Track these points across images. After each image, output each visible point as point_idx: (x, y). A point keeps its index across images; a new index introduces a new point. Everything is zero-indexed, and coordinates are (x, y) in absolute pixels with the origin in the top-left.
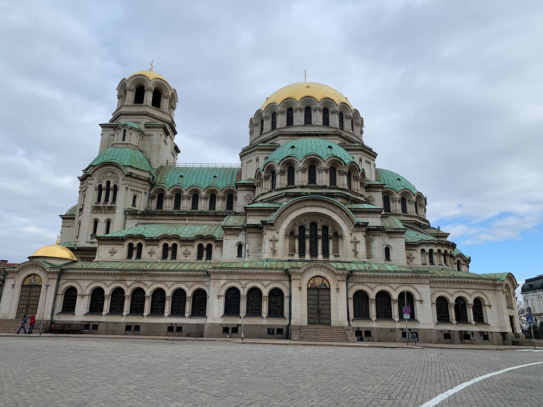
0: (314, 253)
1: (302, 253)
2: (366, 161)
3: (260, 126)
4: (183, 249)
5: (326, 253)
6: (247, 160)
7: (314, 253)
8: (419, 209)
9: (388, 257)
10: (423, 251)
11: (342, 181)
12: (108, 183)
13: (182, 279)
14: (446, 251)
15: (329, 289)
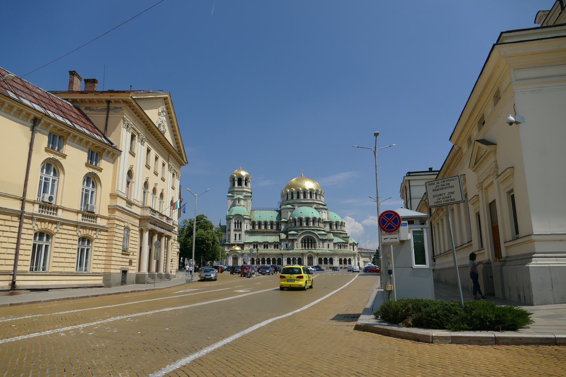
0: (308, 247)
1: (305, 247)
2: (324, 212)
3: (286, 196)
4: (270, 245)
5: (312, 247)
6: (284, 211)
7: (308, 247)
8: (342, 227)
9: (328, 247)
10: (338, 245)
11: (316, 224)
12: (238, 221)
13: (275, 255)
14: (345, 245)
15: (312, 258)
